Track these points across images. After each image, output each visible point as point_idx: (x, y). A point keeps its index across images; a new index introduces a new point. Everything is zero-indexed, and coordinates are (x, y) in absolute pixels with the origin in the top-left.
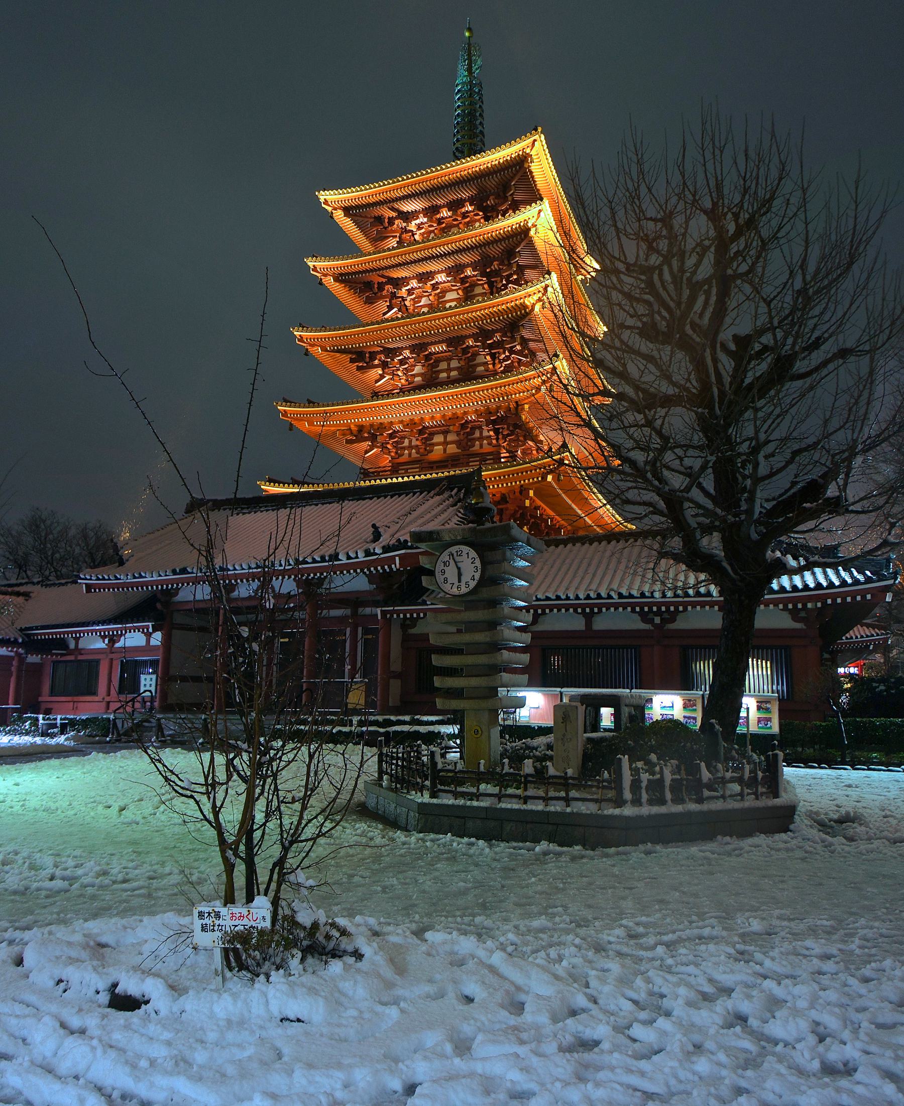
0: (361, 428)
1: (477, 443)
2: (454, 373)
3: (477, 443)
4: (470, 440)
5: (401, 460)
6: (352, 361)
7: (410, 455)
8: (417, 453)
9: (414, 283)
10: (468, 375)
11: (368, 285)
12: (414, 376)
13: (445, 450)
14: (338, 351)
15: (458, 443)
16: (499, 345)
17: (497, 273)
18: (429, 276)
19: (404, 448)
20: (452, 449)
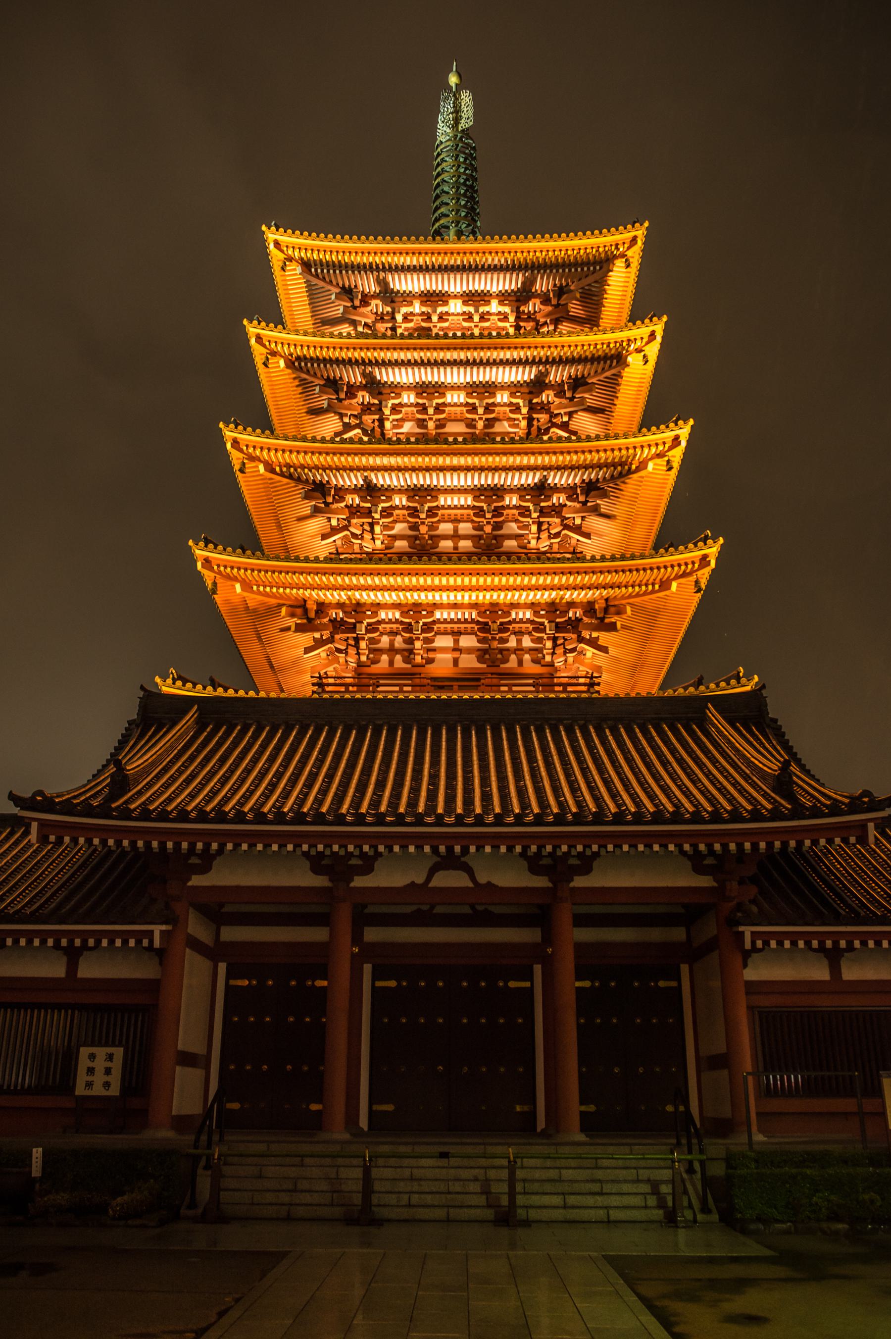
0: (322, 607)
1: (513, 657)
2: (465, 545)
3: (513, 657)
4: (501, 651)
5: (375, 669)
6: (307, 496)
7: (391, 663)
8: (407, 660)
9: (409, 398)
10: (489, 549)
11: (333, 384)
12: (395, 537)
13: (456, 662)
14: (290, 477)
15: (482, 654)
16: (557, 511)
17: (544, 408)
18: (439, 389)
19: (381, 651)
20: (469, 662)
